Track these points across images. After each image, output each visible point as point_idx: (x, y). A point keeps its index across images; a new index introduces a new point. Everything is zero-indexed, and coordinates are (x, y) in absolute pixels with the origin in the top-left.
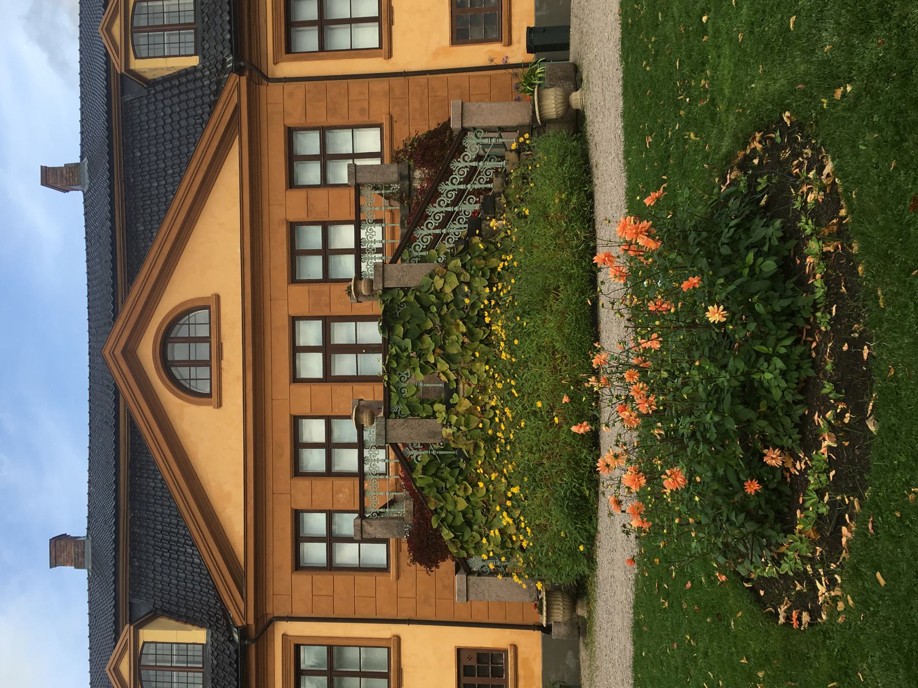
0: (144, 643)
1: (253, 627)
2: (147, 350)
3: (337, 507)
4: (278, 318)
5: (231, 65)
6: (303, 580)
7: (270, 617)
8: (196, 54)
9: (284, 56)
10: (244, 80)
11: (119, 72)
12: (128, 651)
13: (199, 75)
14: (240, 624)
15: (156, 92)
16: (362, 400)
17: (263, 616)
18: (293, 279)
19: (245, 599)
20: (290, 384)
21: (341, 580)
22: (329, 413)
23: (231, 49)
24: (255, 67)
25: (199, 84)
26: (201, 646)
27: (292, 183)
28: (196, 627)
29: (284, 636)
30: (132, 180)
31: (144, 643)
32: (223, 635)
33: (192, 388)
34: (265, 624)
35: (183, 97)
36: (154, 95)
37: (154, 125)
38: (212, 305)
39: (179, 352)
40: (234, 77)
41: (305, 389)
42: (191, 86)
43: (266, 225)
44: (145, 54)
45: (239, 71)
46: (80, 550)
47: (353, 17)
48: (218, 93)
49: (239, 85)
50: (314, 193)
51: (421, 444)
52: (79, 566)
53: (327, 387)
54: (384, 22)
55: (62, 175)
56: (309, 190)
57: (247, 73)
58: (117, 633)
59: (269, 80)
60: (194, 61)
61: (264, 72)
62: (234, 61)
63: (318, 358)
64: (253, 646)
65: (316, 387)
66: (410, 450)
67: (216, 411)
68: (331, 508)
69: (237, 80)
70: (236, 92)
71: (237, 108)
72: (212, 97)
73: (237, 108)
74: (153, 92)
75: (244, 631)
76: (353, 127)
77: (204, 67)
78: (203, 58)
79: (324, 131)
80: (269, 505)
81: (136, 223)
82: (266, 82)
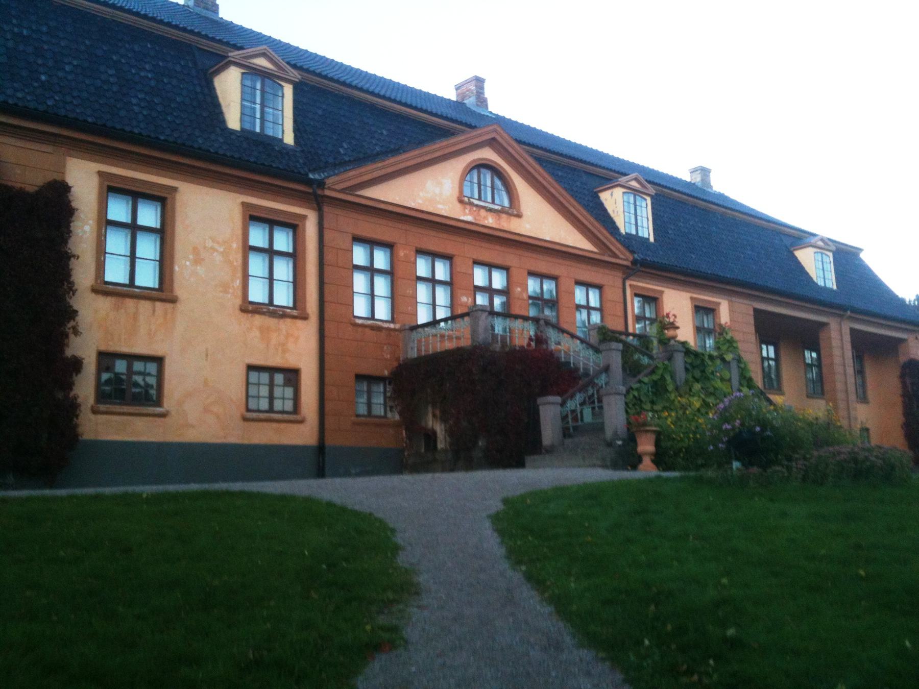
2: (488, 154)
4: (510, 257)
12: (276, 70)
19: (342, 191)
24: (635, 273)
29: (304, 217)
34: (318, 202)
38: (514, 210)
39: (487, 178)
40: (631, 258)
45: (634, 262)
47: (250, 278)
49: (626, 260)
54: (370, 322)
58: (294, 66)
61: (631, 278)
64: (311, 191)
70: (624, 257)
75: (321, 184)
80: (400, 226)
82: (624, 276)
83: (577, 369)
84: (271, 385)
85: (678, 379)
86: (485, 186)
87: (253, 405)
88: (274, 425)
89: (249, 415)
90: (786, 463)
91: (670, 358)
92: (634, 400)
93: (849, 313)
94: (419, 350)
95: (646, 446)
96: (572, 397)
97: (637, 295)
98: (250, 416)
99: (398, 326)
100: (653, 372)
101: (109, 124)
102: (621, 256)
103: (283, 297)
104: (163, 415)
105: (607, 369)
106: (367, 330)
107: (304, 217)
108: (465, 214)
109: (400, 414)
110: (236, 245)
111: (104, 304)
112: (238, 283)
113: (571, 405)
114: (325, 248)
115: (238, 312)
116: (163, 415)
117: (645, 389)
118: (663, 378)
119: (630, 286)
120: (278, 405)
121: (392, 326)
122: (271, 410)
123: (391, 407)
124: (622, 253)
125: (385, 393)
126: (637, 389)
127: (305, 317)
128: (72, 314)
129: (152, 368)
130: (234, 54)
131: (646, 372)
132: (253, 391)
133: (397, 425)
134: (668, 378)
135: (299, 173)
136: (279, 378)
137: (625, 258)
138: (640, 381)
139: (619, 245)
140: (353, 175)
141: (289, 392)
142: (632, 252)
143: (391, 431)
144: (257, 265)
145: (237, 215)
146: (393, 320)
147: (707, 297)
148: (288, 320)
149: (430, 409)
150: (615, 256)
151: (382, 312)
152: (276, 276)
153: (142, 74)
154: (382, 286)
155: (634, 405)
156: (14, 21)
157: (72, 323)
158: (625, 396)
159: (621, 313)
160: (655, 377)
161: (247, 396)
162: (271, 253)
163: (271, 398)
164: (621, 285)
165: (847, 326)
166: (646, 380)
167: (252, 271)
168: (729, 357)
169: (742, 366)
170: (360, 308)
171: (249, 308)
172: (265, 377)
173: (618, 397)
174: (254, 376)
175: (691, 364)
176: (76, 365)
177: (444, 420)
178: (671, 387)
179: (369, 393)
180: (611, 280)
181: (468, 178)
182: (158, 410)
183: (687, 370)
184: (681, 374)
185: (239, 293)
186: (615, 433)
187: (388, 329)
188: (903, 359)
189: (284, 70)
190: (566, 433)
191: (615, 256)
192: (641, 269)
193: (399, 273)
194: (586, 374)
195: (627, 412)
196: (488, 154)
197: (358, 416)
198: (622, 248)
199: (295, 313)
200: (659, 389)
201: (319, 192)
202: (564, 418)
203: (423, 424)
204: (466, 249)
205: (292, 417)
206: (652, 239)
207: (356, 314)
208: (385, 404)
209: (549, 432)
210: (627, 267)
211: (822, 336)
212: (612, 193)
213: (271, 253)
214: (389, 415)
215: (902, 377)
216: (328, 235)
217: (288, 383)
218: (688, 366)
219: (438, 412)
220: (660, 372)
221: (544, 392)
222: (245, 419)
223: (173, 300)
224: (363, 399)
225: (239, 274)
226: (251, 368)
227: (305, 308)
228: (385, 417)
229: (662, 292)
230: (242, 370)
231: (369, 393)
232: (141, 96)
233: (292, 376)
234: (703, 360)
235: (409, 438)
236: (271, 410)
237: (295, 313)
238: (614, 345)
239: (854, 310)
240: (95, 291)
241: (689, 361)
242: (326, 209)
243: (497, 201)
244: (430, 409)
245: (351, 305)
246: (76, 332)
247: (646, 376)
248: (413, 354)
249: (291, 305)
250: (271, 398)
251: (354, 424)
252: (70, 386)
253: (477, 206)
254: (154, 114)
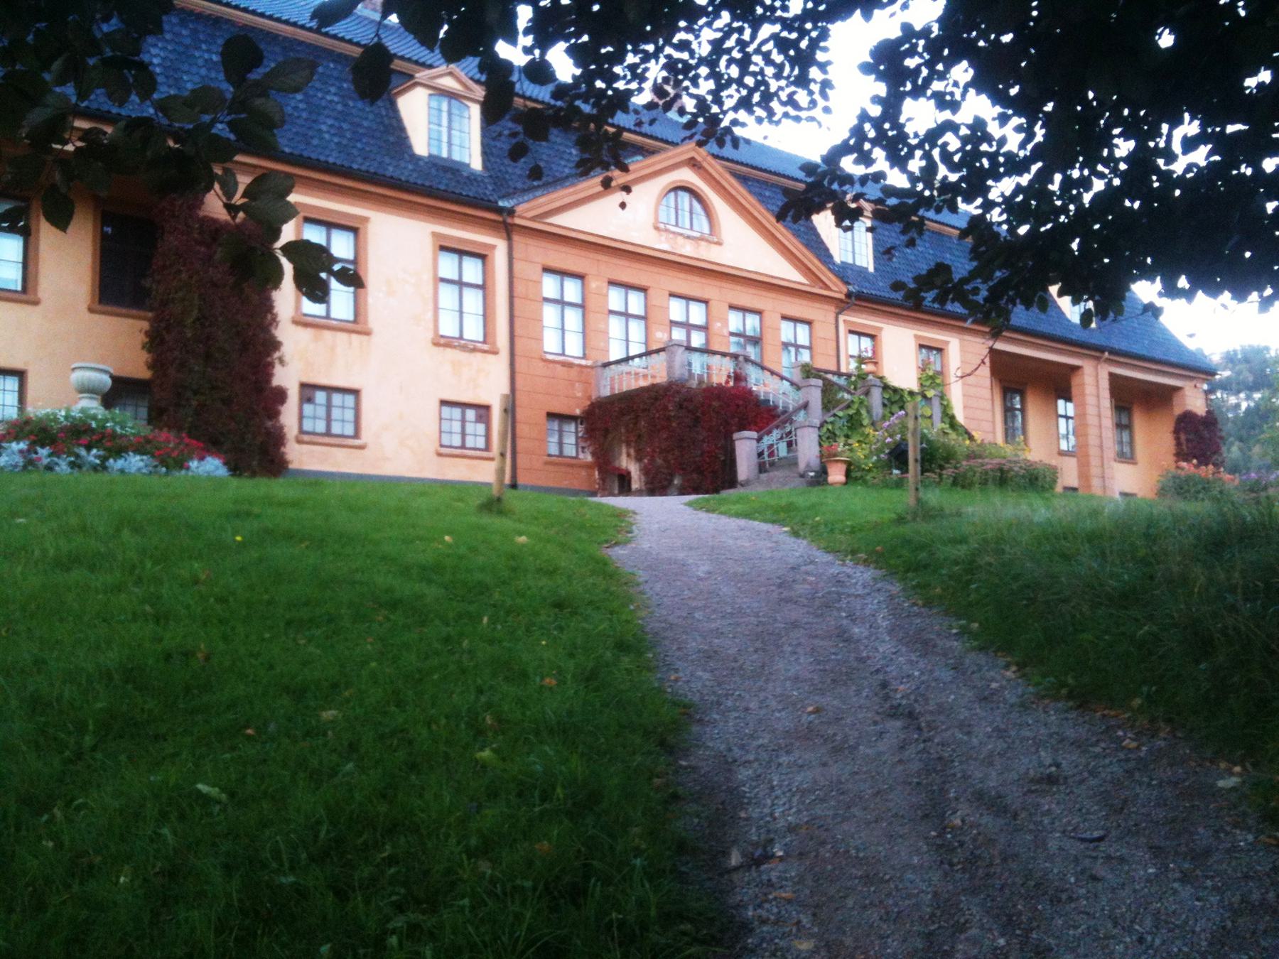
3: (592, 317)
19: (533, 219)
29: (493, 247)
34: (508, 230)
38: (713, 236)
40: (844, 289)
45: (849, 295)
49: (841, 292)
59: (837, 314)
64: (500, 219)
75: (511, 212)
83: (776, 407)
84: (463, 421)
85: (874, 414)
86: (683, 210)
87: (445, 442)
88: (466, 461)
89: (444, 450)
90: (938, 471)
91: (867, 393)
92: (828, 434)
93: (1107, 354)
94: (612, 388)
95: (836, 475)
96: (769, 433)
97: (851, 332)
98: (444, 452)
99: (589, 363)
100: (848, 407)
101: (305, 154)
102: (834, 288)
103: (474, 331)
104: (362, 447)
105: (805, 406)
106: (558, 367)
107: (493, 247)
109: (593, 454)
110: (427, 277)
111: (305, 334)
112: (430, 315)
113: (767, 440)
114: (515, 280)
115: (430, 345)
116: (362, 447)
117: (839, 423)
118: (858, 413)
119: (844, 321)
120: (470, 442)
121: (583, 362)
122: (463, 447)
123: (583, 448)
124: (836, 286)
125: (577, 432)
126: (832, 423)
127: (495, 353)
128: (275, 345)
129: (350, 400)
130: (422, 75)
131: (841, 406)
132: (445, 426)
133: (588, 467)
134: (863, 412)
135: (489, 201)
136: (471, 414)
137: (838, 290)
138: (835, 415)
139: (831, 276)
140: (544, 201)
141: (481, 428)
142: (847, 283)
143: (584, 473)
144: (448, 295)
145: (428, 245)
146: (584, 357)
147: (934, 335)
148: (479, 355)
149: (624, 450)
150: (827, 288)
151: (574, 348)
152: (441, 305)
153: (329, 98)
154: (573, 317)
155: (828, 437)
156: (204, 47)
157: (277, 355)
158: (819, 428)
159: (833, 353)
160: (851, 412)
161: (441, 432)
162: (460, 284)
163: (463, 434)
164: (833, 321)
165: (1104, 371)
166: (841, 414)
167: (442, 304)
168: (930, 393)
169: (945, 403)
170: (551, 344)
171: (442, 342)
172: (457, 412)
173: (810, 429)
174: (446, 410)
175: (889, 399)
176: (281, 395)
177: (639, 459)
178: (865, 422)
179: (561, 432)
180: (822, 314)
181: (664, 202)
182: (357, 442)
183: (884, 405)
184: (878, 409)
185: (431, 326)
186: (808, 465)
187: (580, 366)
188: (1178, 411)
189: (471, 90)
190: (762, 468)
191: (827, 287)
193: (591, 305)
194: (785, 412)
195: (820, 445)
196: (686, 175)
197: (550, 455)
199: (486, 347)
200: (854, 423)
201: (509, 220)
202: (760, 454)
203: (617, 464)
204: (663, 281)
205: (485, 454)
206: (871, 269)
207: (546, 349)
208: (577, 444)
209: (745, 465)
210: (841, 300)
211: (1075, 381)
213: (460, 284)
214: (581, 456)
215: (1176, 431)
216: (518, 266)
217: (479, 419)
218: (886, 402)
219: (632, 451)
220: (856, 406)
221: (742, 428)
222: (440, 455)
223: (367, 333)
224: (555, 439)
225: (431, 306)
226: (444, 403)
227: (494, 343)
228: (576, 458)
229: (880, 329)
230: (437, 404)
231: (561, 432)
232: (330, 122)
233: (483, 411)
234: (902, 396)
235: (603, 479)
236: (463, 447)
237: (486, 347)
238: (813, 381)
239: (1113, 352)
240: (296, 322)
241: (887, 396)
242: (516, 238)
243: (695, 227)
244: (624, 450)
245: (540, 340)
246: (281, 361)
247: (841, 410)
248: (606, 392)
249: (481, 339)
250: (463, 434)
251: (547, 463)
252: (275, 414)
253: (674, 233)
254: (345, 142)
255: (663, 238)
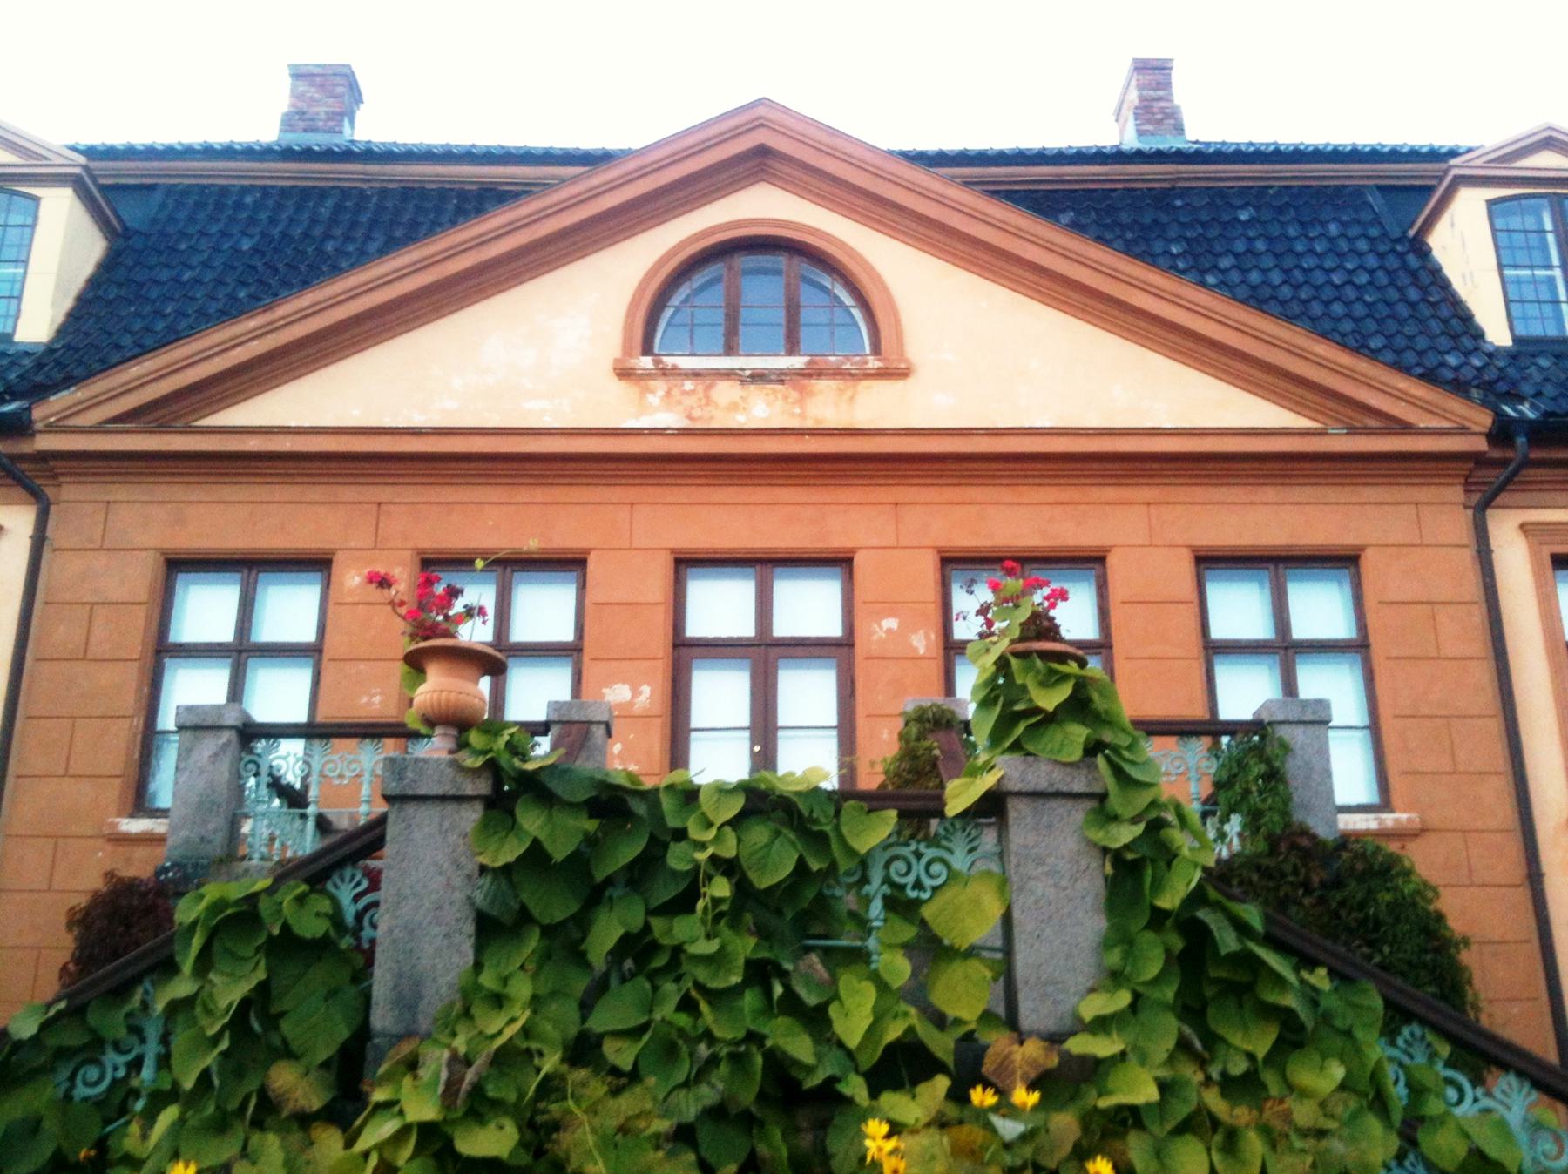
0: (36, 200)
1: (26, 447)
5: (1513, 414)
6: (138, 576)
7: (50, 492)
8: (1516, 340)
9: (1546, 551)
10: (1481, 445)
11: (1453, 162)
12: (23, 162)
13: (1467, 343)
14: (37, 413)
15: (1401, 255)
16: (609, 734)
17: (55, 476)
18: (955, 563)
19: (100, 429)
20: (673, 551)
21: (125, 681)
22: (588, 651)
23: (1552, 414)
24: (1515, 473)
25: (1444, 343)
26: (9, 330)
27: (1210, 561)
28: (60, 319)
30: (1179, 203)
31: (36, 200)
32: (21, 377)
33: (668, 313)
35: (1403, 310)
36: (1393, 251)
37: (1318, 249)
40: (1484, 420)
41: (656, 585)
42: (1435, 326)
43: (1097, 493)
44: (1500, 224)
45: (1501, 433)
46: (320, 124)
48: (1430, 377)
49: (1463, 431)
50: (1190, 614)
51: (373, 942)
52: (288, 123)
53: (660, 643)
55: (1160, 99)
56: (1195, 608)
57: (1496, 454)
60: (1498, 334)
61: (1503, 498)
62: (1523, 420)
63: (745, 627)
65: (660, 620)
66: (356, 898)
67: (608, 365)
68: (326, 656)
69: (1476, 428)
70: (1446, 424)
71: (1406, 428)
72: (1419, 370)
73: (1406, 428)
74: (1399, 248)
76: (1374, 728)
77: (1490, 355)
78: (1513, 356)
79: (1358, 647)
81: (1073, 209)
102: (1424, 421)
108: (644, 409)
159: (1478, 645)
192: (1533, 455)
198: (1419, 390)
210: (1477, 459)
212: (1452, 218)
253: (696, 374)
255: (654, 399)
